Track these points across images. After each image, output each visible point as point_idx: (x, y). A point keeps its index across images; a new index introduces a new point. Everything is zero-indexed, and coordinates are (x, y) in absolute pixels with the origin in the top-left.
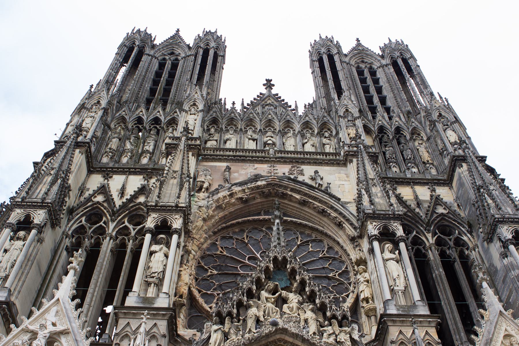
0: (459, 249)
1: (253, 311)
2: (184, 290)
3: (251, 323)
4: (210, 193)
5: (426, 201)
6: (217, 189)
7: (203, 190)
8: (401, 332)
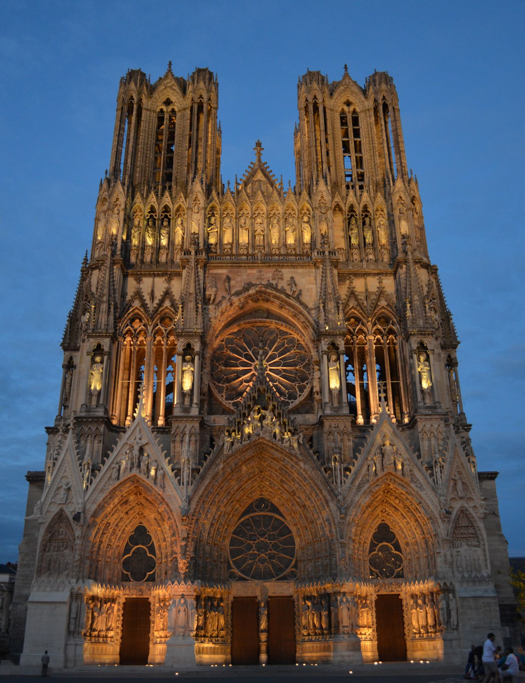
2: (206, 389)
4: (216, 305)
5: (374, 293)
6: (220, 301)
7: (211, 302)
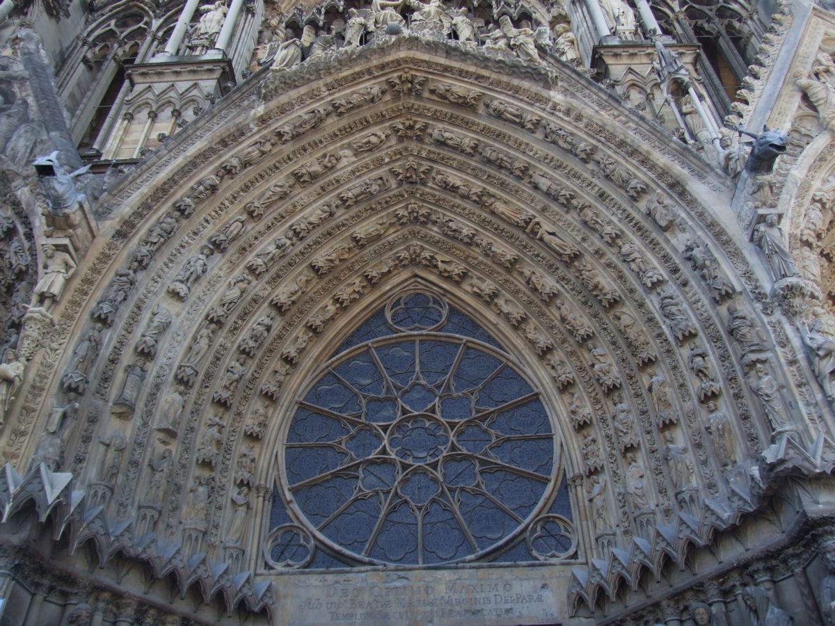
0: (726, 22)
1: (357, 20)
3: (353, 34)
8: (630, 71)
